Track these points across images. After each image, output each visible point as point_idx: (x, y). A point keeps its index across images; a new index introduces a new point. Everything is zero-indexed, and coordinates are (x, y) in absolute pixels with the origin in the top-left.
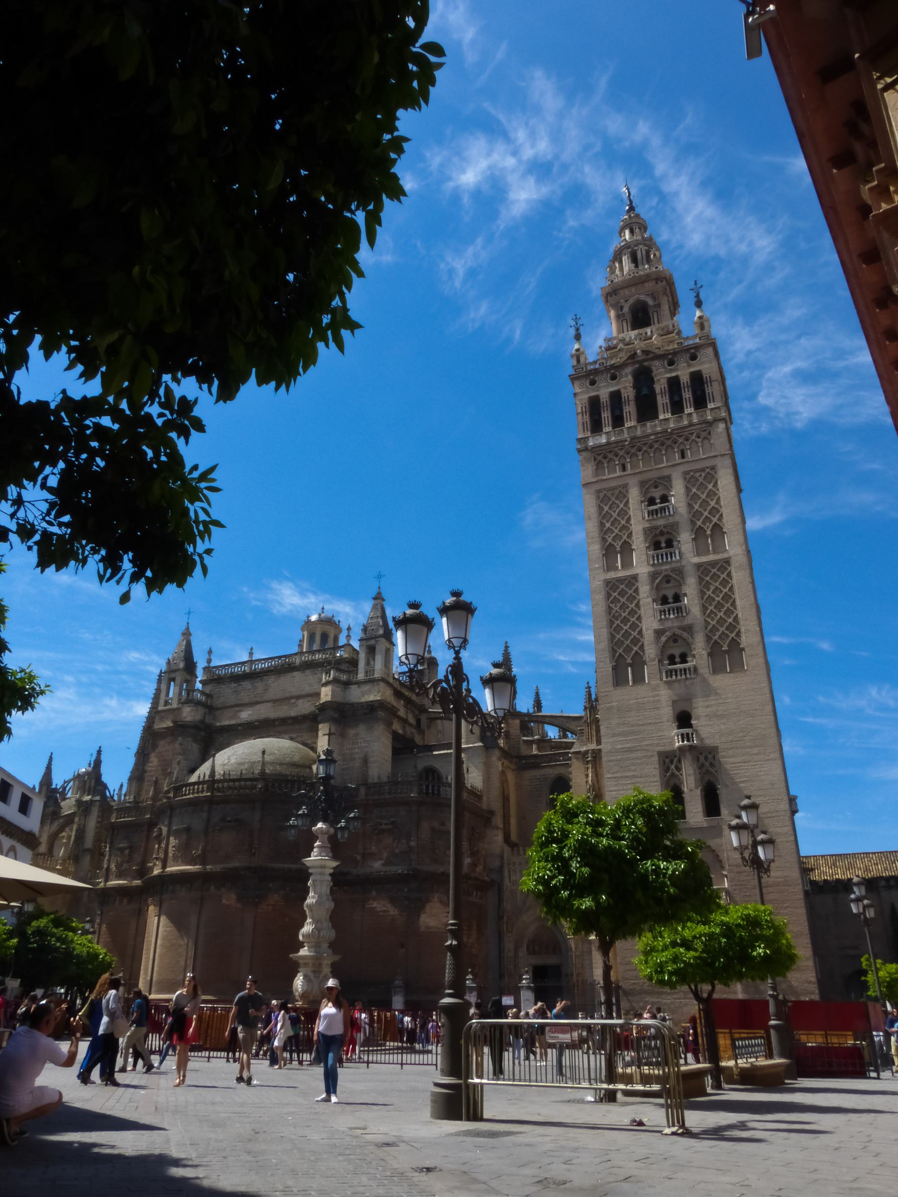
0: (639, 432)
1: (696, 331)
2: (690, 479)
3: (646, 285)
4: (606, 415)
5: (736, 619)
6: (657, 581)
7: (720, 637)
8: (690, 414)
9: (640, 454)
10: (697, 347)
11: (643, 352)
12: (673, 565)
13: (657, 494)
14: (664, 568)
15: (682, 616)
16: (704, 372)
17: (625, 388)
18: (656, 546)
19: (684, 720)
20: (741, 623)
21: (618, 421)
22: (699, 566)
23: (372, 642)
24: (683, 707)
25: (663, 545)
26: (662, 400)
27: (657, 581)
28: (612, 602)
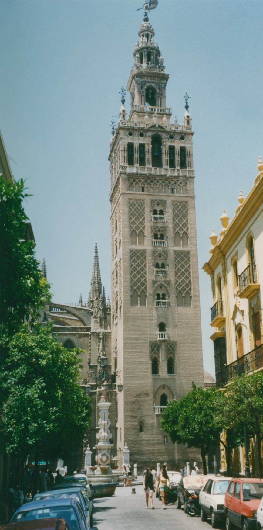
0: (153, 172)
1: (185, 124)
2: (175, 206)
5: (190, 282)
7: (182, 289)
8: (178, 170)
9: (152, 184)
10: (186, 134)
13: (158, 208)
16: (187, 148)
18: (156, 236)
19: (162, 327)
20: (192, 284)
22: (175, 252)
24: (163, 320)
25: (159, 236)
26: (165, 158)
28: (133, 262)
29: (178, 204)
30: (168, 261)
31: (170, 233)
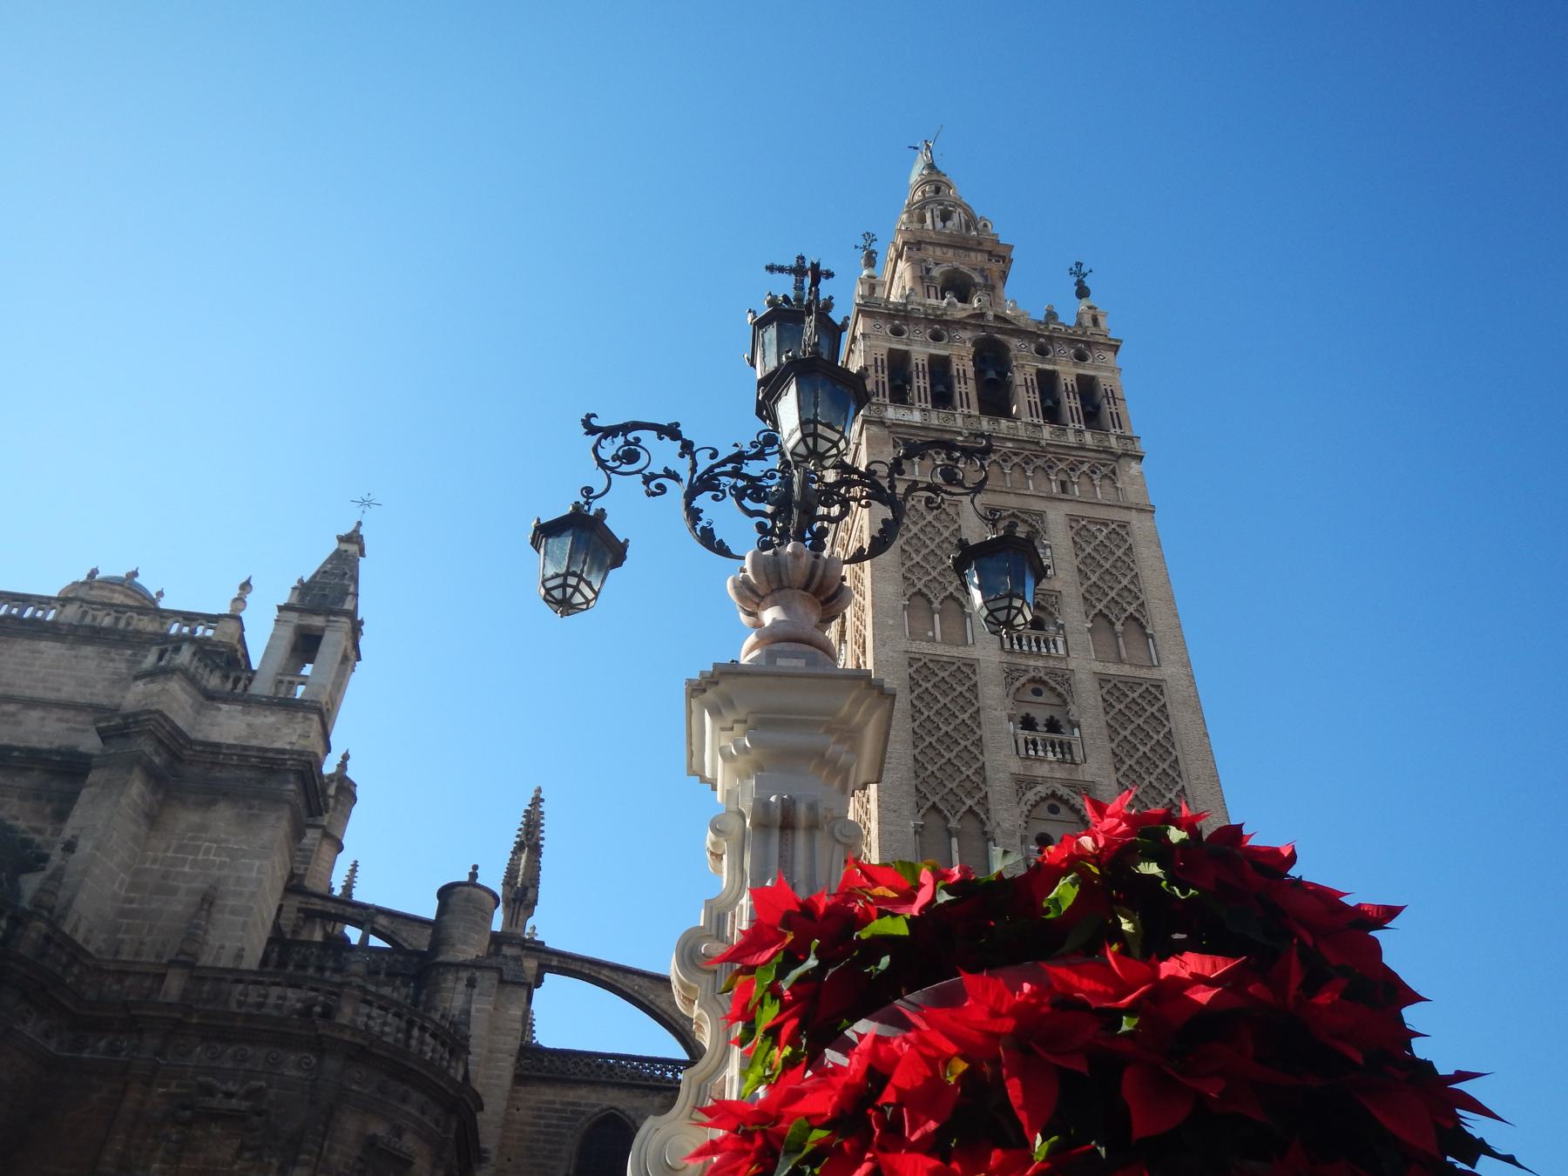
2: (1080, 529)
3: (973, 254)
4: (921, 384)
6: (1018, 684)
8: (1080, 432)
11: (996, 317)
12: (1051, 663)
14: (1032, 663)
15: (1073, 762)
17: (961, 358)
21: (942, 398)
22: (1103, 680)
23: (318, 621)
26: (1024, 401)
27: (1018, 684)
28: (919, 697)
29: (1093, 528)
30: (1073, 709)
31: (1073, 615)
